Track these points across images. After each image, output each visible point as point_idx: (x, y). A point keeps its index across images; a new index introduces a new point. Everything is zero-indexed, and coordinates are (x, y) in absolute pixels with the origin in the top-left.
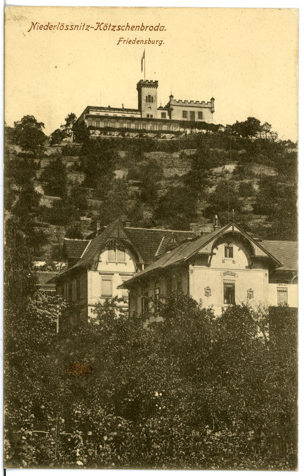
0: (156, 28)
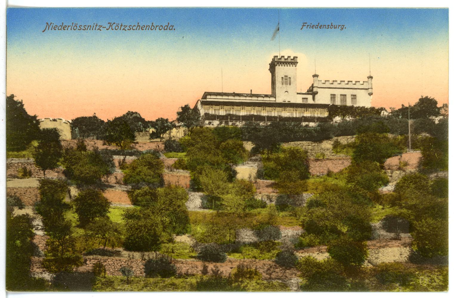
0: (166, 28)
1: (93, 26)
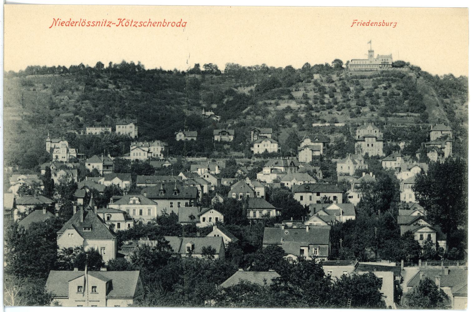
0: (178, 24)
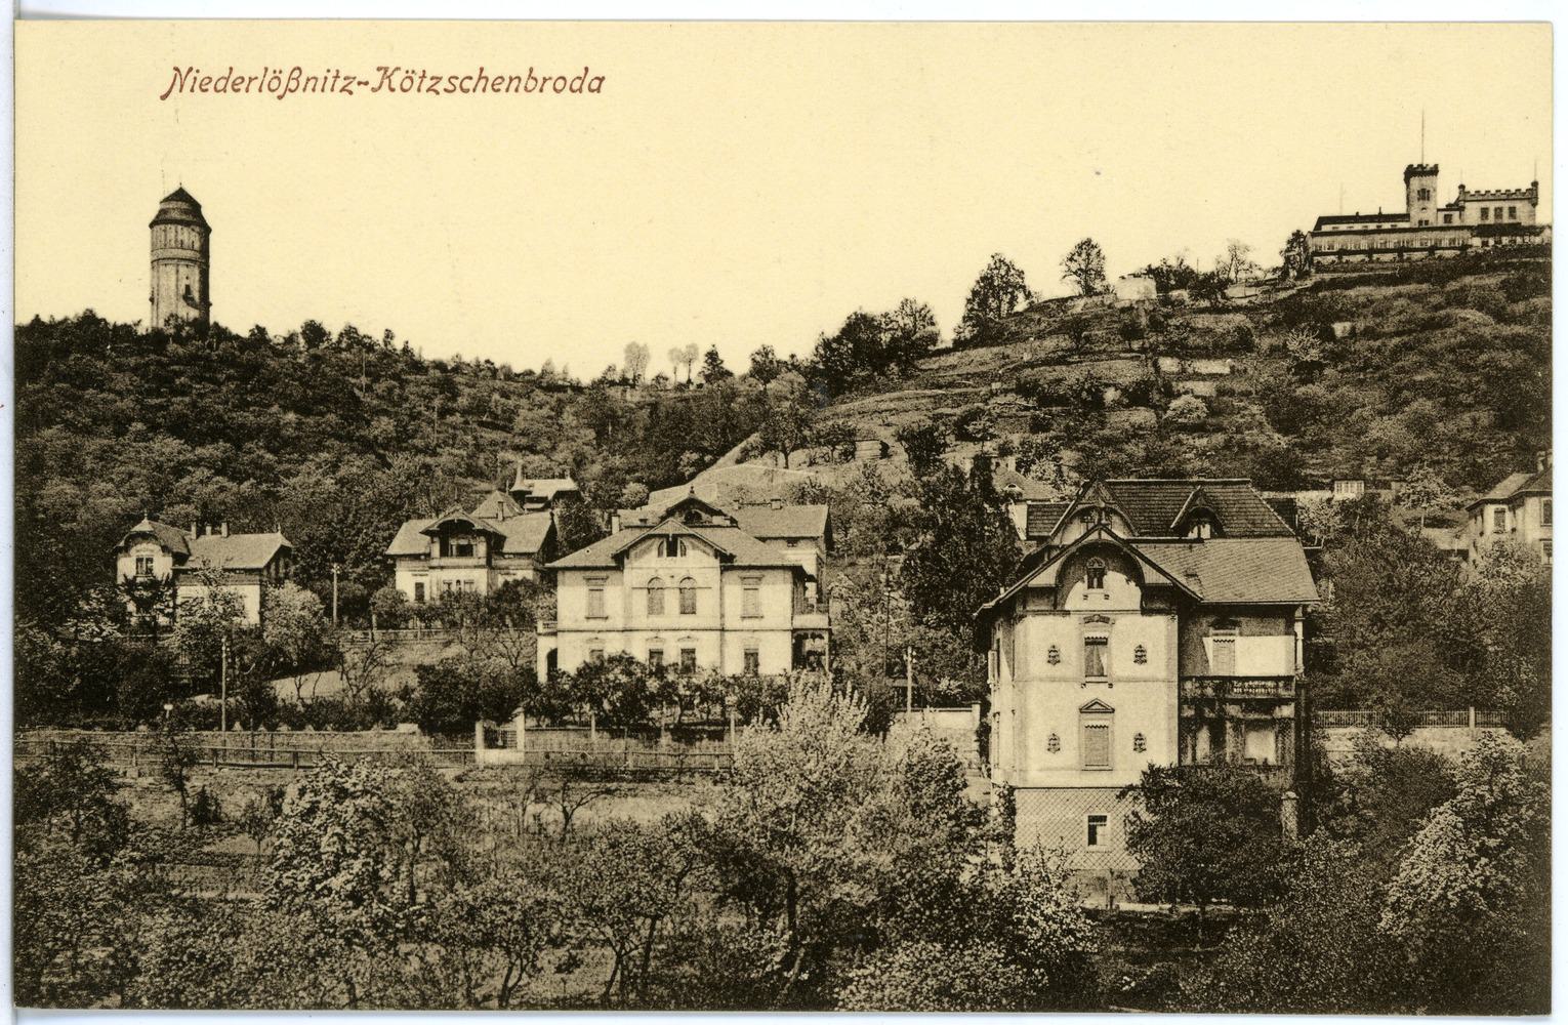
0: (576, 85)
1: (326, 78)
